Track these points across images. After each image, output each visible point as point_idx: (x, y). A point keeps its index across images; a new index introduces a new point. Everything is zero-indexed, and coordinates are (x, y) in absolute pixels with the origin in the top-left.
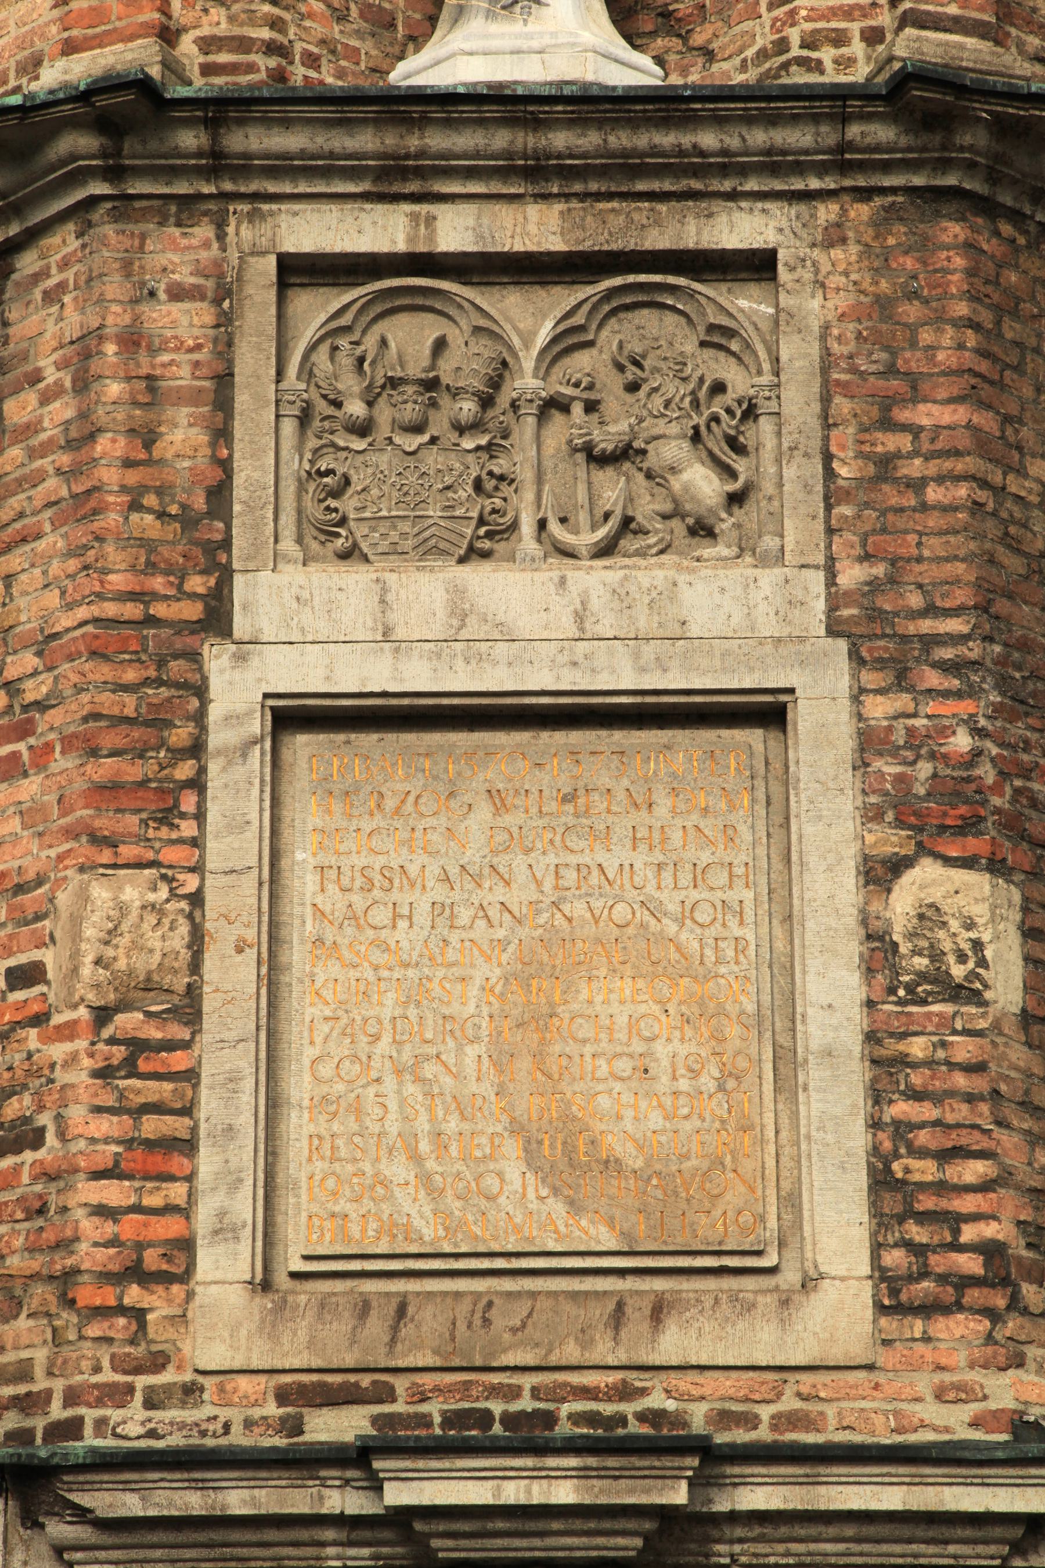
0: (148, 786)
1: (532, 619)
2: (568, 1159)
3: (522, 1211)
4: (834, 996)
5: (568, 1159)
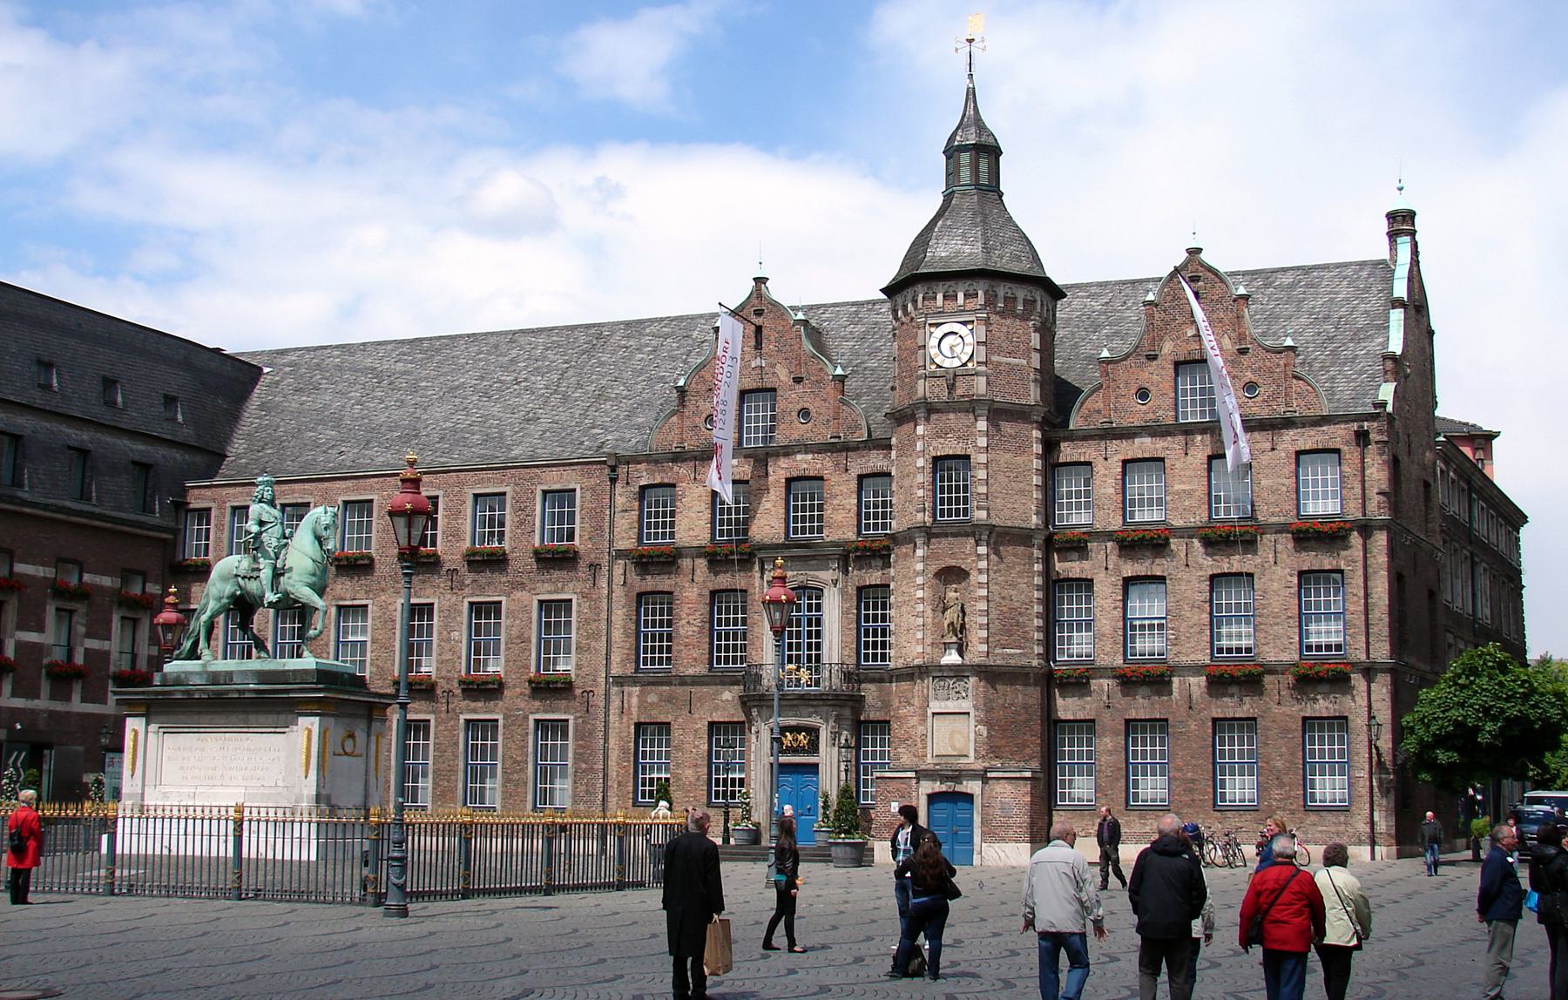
1: (951, 706)
2: (953, 747)
4: (972, 736)
5: (953, 747)
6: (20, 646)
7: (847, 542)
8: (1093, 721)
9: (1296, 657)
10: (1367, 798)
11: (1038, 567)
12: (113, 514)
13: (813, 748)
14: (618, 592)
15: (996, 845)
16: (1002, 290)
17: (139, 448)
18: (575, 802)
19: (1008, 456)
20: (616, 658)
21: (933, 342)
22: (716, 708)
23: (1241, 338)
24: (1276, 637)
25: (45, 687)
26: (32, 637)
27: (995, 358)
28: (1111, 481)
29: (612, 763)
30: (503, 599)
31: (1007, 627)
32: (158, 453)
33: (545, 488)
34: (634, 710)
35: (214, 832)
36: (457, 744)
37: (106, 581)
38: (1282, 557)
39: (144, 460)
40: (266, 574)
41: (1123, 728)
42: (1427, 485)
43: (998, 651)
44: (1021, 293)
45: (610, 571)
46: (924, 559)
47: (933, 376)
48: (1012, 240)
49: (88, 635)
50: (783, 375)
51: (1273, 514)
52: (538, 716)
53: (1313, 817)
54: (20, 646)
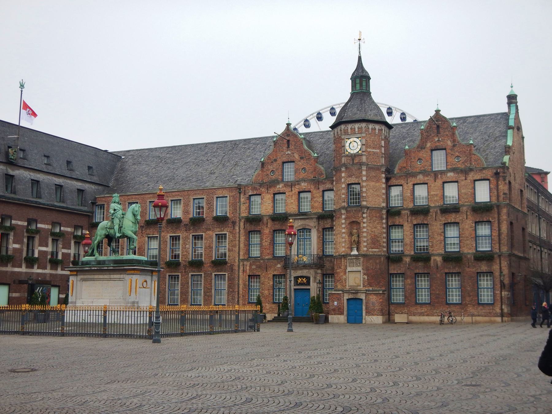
0: (345, 273)
1: (355, 269)
2: (356, 283)
3: (355, 284)
4: (362, 279)
5: (356, 283)
6: (40, 252)
7: (318, 213)
8: (403, 274)
9: (474, 251)
10: (500, 300)
11: (384, 221)
12: (71, 207)
13: (308, 283)
14: (242, 231)
15: (370, 317)
16: (371, 126)
17: (79, 185)
18: (228, 302)
19: (373, 183)
20: (241, 253)
21: (347, 145)
22: (275, 270)
23: (454, 141)
24: (467, 245)
25: (49, 266)
26: (44, 249)
27: (369, 150)
28: (409, 191)
29: (241, 289)
30: (204, 234)
31: (375, 242)
32: (86, 186)
33: (217, 196)
34: (248, 271)
35: (100, 314)
37: (69, 230)
38: (469, 217)
39: (81, 188)
40: (116, 227)
41: (414, 276)
42: (521, 191)
43: (370, 250)
44: (377, 127)
45: (239, 224)
46: (345, 219)
47: (347, 156)
48: (374, 109)
49: (63, 248)
50: (297, 156)
51: (466, 202)
52: (216, 273)
53: (481, 307)
54: (40, 252)
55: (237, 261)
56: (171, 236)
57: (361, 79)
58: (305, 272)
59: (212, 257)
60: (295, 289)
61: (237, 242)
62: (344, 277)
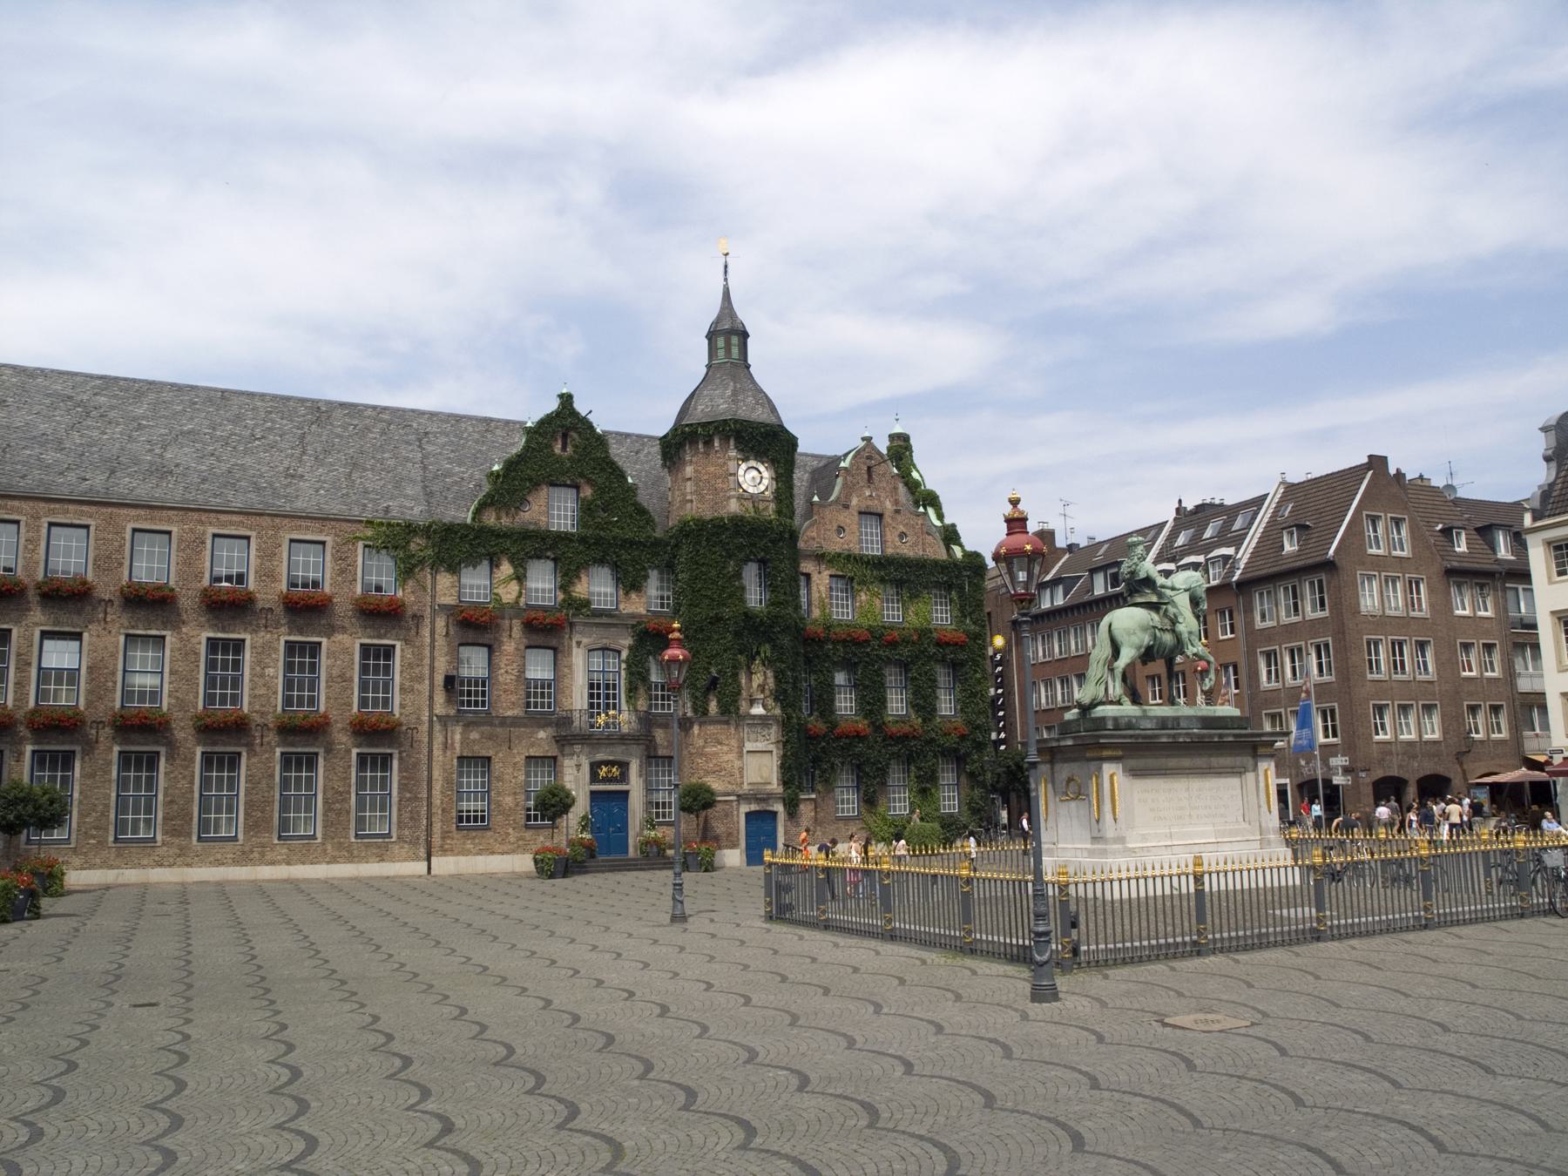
0: (740, 756)
1: (760, 746)
13: (623, 778)
14: (440, 642)
22: (532, 745)
30: (324, 641)
34: (457, 746)
36: (272, 776)
45: (433, 623)
55: (425, 719)
56: (209, 639)
57: (728, 337)
58: (616, 754)
59: (350, 705)
60: (592, 793)
61: (427, 672)
62: (737, 763)
